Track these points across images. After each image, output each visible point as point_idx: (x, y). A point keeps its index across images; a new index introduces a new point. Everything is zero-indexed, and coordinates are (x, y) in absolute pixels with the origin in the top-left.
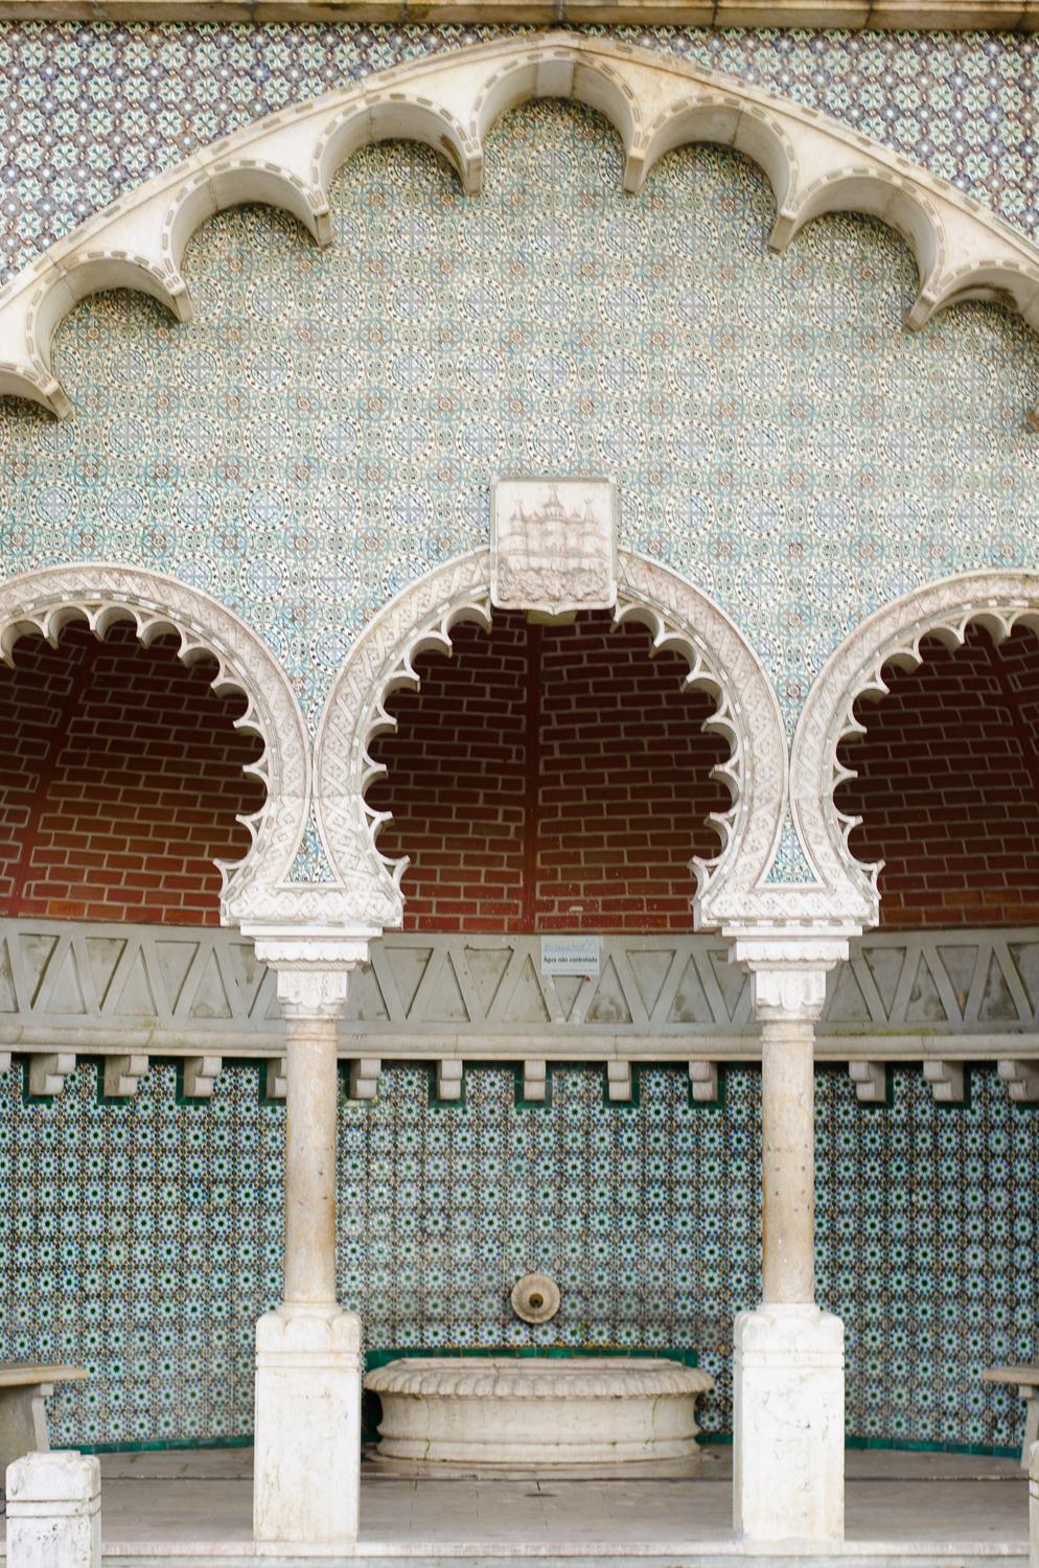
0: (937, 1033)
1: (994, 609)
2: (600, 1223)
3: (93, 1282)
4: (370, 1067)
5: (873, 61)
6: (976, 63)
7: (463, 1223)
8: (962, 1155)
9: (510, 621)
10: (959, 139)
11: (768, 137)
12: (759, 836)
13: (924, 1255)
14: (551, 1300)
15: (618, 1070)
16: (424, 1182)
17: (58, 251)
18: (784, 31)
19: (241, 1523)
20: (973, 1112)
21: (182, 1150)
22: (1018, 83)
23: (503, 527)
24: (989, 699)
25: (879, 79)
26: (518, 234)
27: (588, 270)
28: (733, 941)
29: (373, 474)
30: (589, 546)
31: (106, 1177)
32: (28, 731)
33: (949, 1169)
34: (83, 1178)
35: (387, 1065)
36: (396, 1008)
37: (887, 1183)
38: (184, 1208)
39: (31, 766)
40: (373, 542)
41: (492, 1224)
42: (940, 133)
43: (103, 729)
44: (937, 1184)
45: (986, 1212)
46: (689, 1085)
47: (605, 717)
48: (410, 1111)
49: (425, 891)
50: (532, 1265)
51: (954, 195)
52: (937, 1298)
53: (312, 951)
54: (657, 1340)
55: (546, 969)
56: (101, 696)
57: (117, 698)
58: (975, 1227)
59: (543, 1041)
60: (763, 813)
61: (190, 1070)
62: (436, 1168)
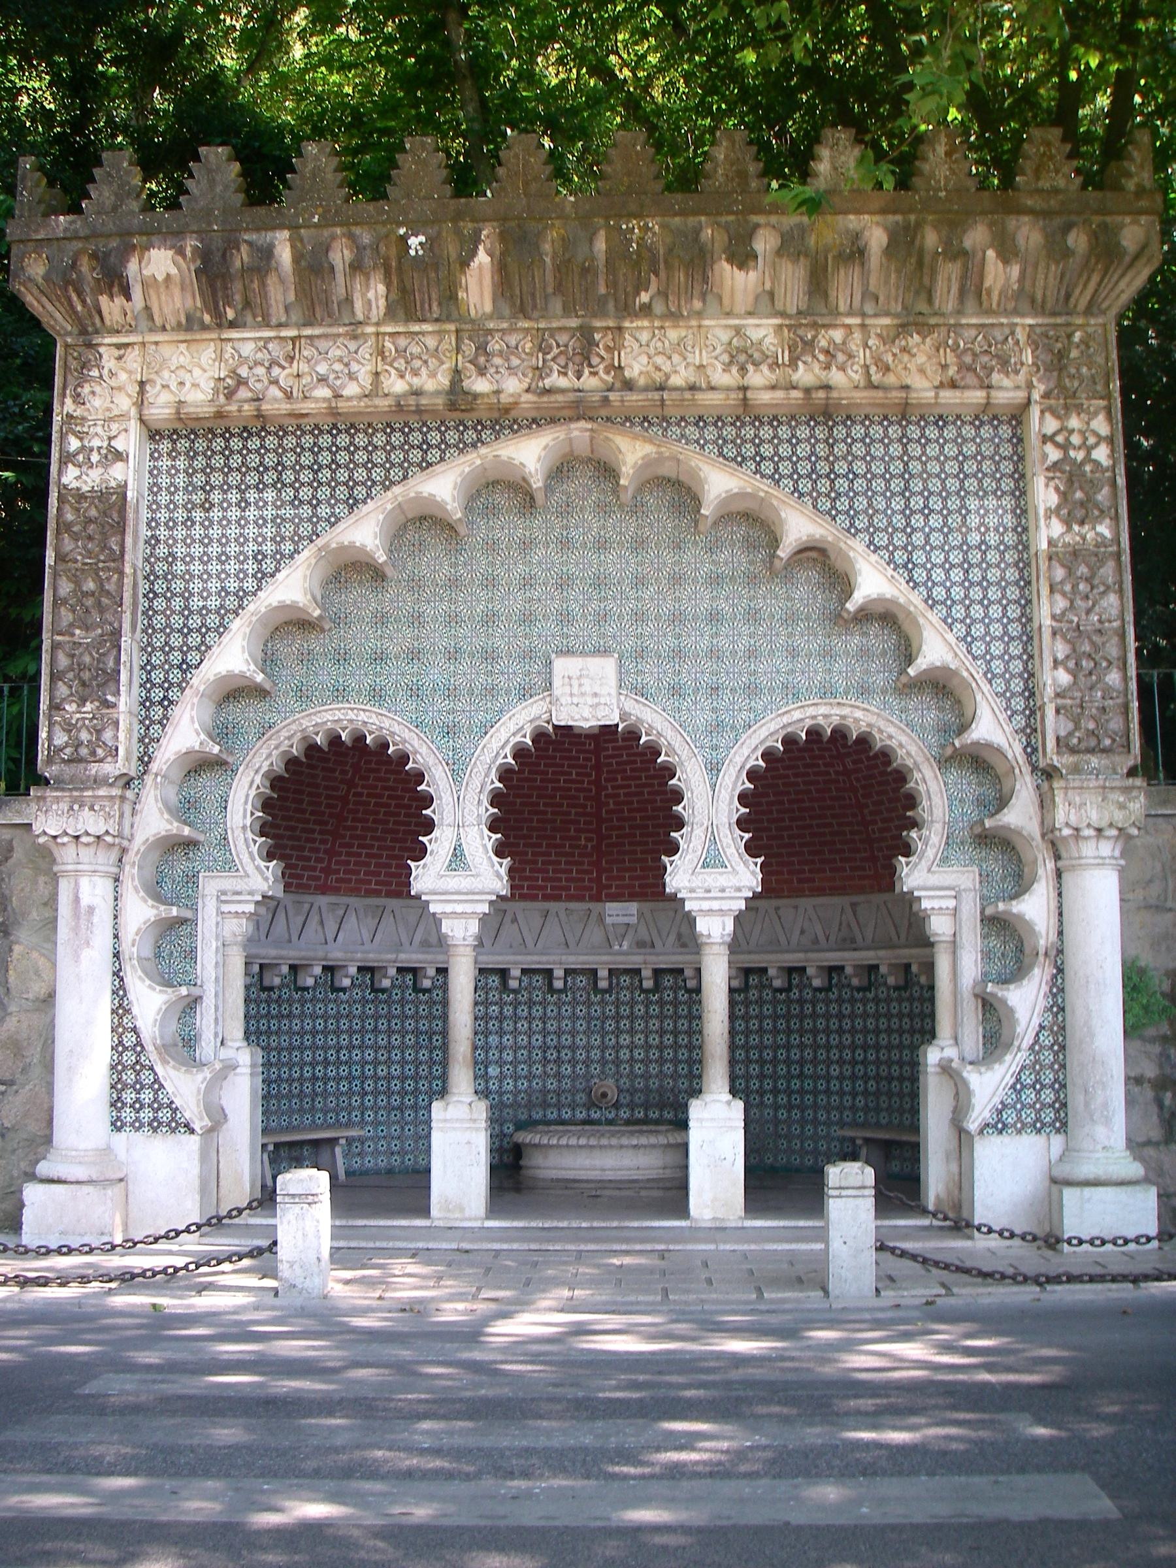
0: (812, 951)
1: (821, 721)
2: (639, 1054)
3: (369, 1086)
4: (515, 972)
5: (748, 431)
6: (803, 432)
7: (566, 1055)
8: (827, 1016)
10: (795, 471)
11: (694, 473)
13: (808, 1069)
14: (613, 1095)
15: (647, 973)
16: (545, 1033)
19: (424, 1210)
21: (416, 1017)
22: (826, 441)
23: (557, 682)
24: (837, 773)
25: (752, 441)
27: (602, 545)
28: (683, 900)
29: (490, 656)
30: (604, 691)
32: (328, 797)
33: (821, 1024)
34: (363, 1031)
35: (524, 971)
36: (530, 942)
37: (789, 1031)
38: (417, 1047)
39: (331, 815)
41: (581, 1055)
42: (785, 468)
43: (369, 795)
44: (815, 1032)
45: (841, 1047)
46: (684, 981)
47: (637, 786)
48: (538, 996)
49: (521, 879)
50: (603, 1075)
52: (815, 1092)
53: (459, 908)
55: (608, 920)
56: (367, 778)
57: (376, 779)
58: (835, 1054)
59: (605, 958)
60: (699, 833)
61: (420, 974)
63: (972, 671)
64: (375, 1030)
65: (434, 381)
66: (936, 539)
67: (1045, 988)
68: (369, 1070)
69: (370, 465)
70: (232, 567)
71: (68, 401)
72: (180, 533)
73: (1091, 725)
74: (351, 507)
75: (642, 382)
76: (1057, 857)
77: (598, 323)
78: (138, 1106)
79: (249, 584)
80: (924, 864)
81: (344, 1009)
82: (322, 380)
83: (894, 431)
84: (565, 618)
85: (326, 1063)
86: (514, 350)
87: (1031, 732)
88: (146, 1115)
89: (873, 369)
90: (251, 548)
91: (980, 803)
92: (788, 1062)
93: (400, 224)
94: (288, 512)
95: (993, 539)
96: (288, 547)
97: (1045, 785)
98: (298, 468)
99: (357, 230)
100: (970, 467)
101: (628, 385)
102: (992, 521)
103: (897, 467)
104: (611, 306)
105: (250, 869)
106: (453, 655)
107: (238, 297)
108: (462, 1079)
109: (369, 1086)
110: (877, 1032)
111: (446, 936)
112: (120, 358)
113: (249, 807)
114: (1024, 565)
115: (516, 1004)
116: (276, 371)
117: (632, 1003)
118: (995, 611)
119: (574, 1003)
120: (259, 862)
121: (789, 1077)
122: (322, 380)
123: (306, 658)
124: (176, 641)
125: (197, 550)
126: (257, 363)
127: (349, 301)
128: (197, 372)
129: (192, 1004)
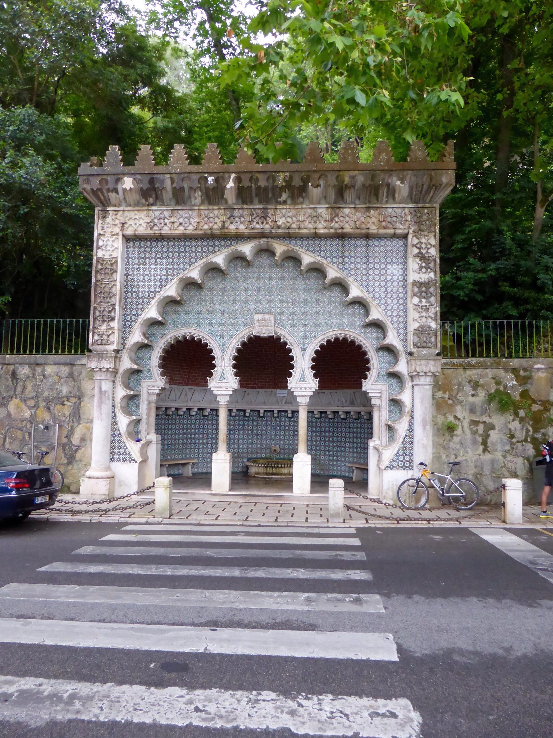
1: (338, 336)
3: (201, 446)
4: (248, 411)
5: (317, 242)
6: (335, 243)
7: (264, 437)
8: (346, 428)
9: (257, 338)
11: (300, 255)
12: (298, 374)
13: (339, 444)
15: (289, 412)
16: (257, 430)
17: (180, 276)
18: (302, 238)
23: (255, 322)
26: (259, 272)
27: (270, 278)
31: (203, 428)
33: (343, 430)
34: (199, 429)
35: (251, 411)
37: (333, 432)
40: (234, 324)
44: (341, 432)
45: (349, 437)
48: (255, 418)
50: (275, 444)
51: (330, 265)
53: (223, 393)
55: (278, 395)
58: (347, 440)
60: (298, 370)
62: (259, 428)
63: (387, 321)
64: (203, 428)
65: (216, 224)
66: (377, 278)
67: (407, 424)
68: (201, 441)
69: (196, 252)
70: (152, 283)
71: (100, 228)
72: (136, 272)
73: (425, 339)
74: (190, 265)
75: (283, 226)
76: (412, 381)
77: (269, 207)
78: (119, 454)
79: (158, 289)
80: (370, 382)
81: (193, 422)
82: (181, 224)
83: (364, 242)
84: (258, 301)
85: (187, 439)
86: (242, 216)
87: (405, 340)
88: (122, 457)
89: (358, 223)
90: (158, 277)
91: (390, 363)
93: (205, 173)
94: (170, 266)
95: (395, 278)
96: (170, 278)
97: (409, 358)
98: (173, 252)
99: (192, 175)
100: (389, 254)
101: (279, 227)
102: (395, 272)
103: (364, 254)
104: (274, 201)
105: (158, 379)
106: (223, 313)
107: (154, 196)
108: (222, 446)
109: (201, 446)
110: (361, 433)
111: (218, 402)
112: (116, 215)
113: (158, 360)
114: (405, 287)
115: (248, 421)
116: (166, 221)
117: (285, 422)
118: (395, 301)
119: (267, 421)
120: (160, 377)
121: (333, 446)
122: (181, 224)
123: (177, 312)
124: (134, 307)
125: (141, 278)
126: (160, 218)
127: (189, 197)
128: (141, 221)
129: (138, 422)
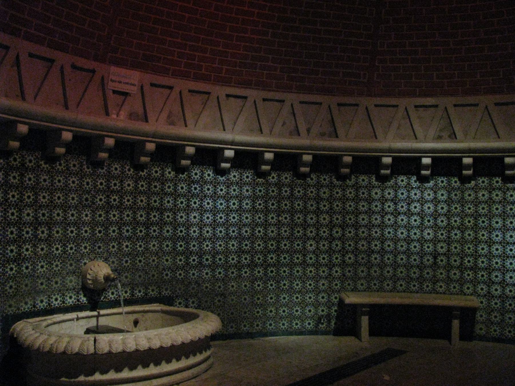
20: (312, 179)
45: (318, 226)
54: (152, 293)
55: (111, 86)
58: (311, 232)
92: (265, 238)
